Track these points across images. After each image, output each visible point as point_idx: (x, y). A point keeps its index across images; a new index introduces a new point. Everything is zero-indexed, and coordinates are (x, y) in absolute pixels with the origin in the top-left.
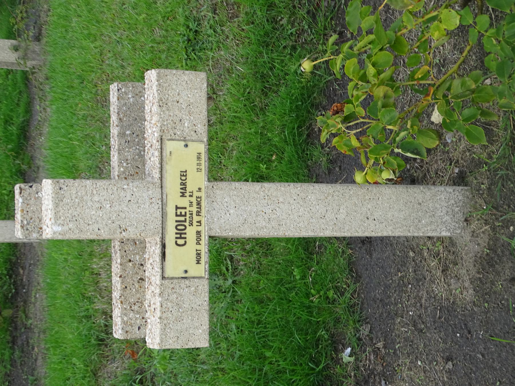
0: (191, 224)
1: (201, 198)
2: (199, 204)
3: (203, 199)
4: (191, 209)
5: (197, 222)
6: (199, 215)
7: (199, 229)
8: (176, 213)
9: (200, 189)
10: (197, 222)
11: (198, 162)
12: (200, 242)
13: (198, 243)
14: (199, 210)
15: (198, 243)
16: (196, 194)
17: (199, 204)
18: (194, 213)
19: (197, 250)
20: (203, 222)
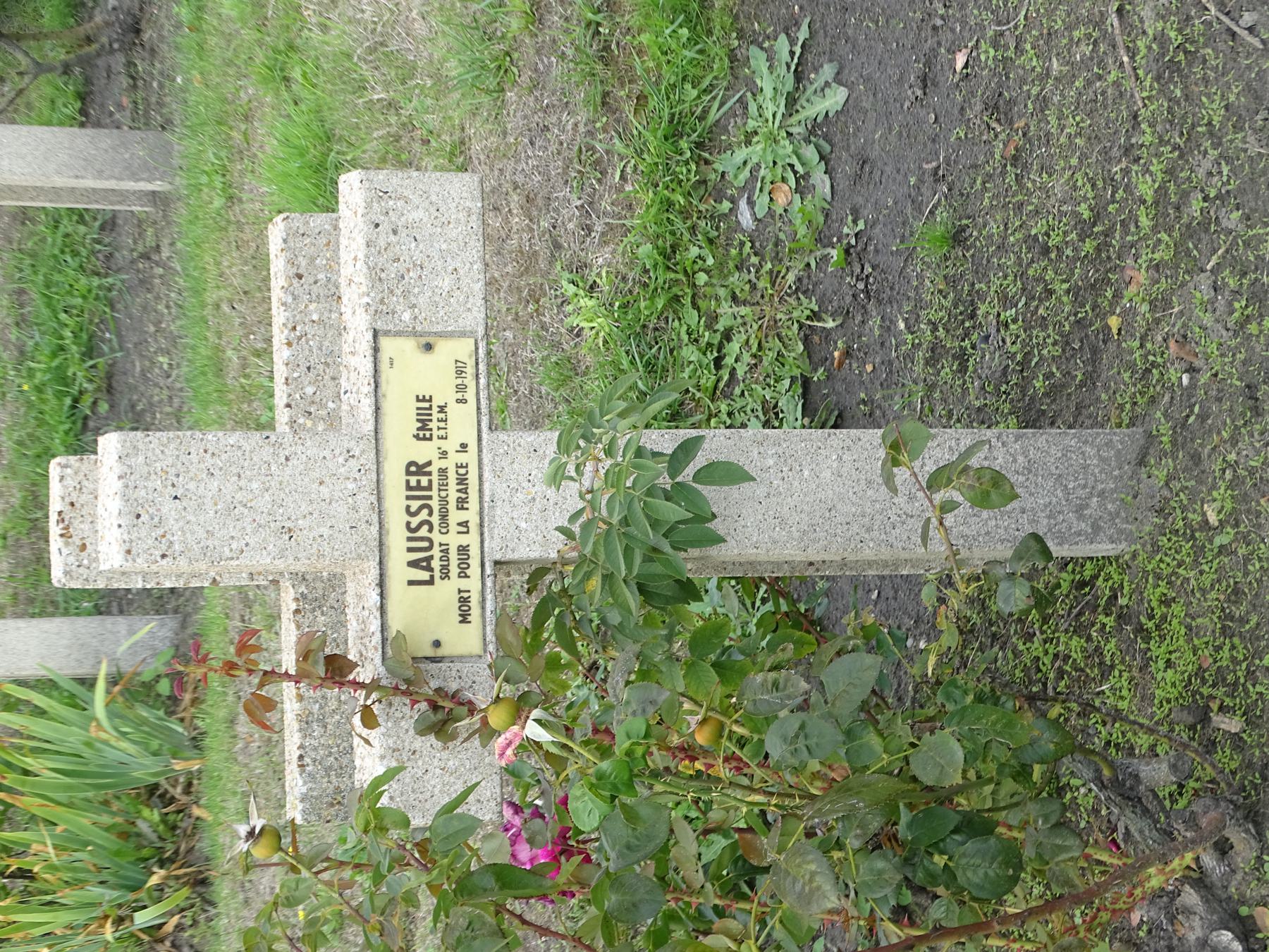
1: (467, 466)
2: (462, 480)
5: (459, 524)
6: (463, 508)
8: (408, 482)
9: (464, 446)
10: (459, 524)
11: (459, 381)
12: (468, 572)
13: (463, 575)
14: (464, 496)
15: (463, 575)
17: (462, 480)
18: (452, 506)
19: (460, 591)
20: (473, 526)
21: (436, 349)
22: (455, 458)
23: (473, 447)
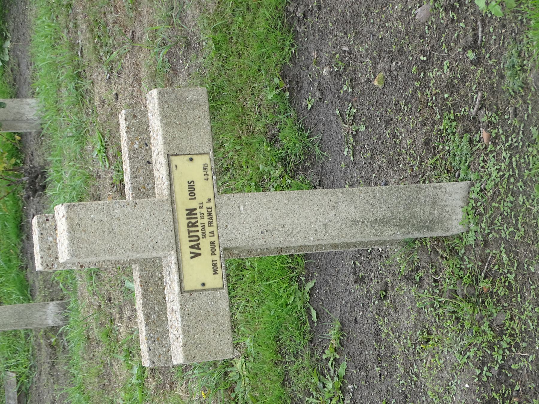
0: (204, 236)
2: (210, 214)
3: (213, 209)
4: (202, 221)
5: (210, 233)
6: (211, 226)
7: (213, 239)
10: (210, 233)
11: (205, 173)
13: (213, 253)
14: (211, 221)
16: (206, 205)
17: (210, 214)
18: (206, 225)
19: (212, 261)
20: (215, 233)
21: (194, 161)
22: (206, 205)
23: (212, 200)
